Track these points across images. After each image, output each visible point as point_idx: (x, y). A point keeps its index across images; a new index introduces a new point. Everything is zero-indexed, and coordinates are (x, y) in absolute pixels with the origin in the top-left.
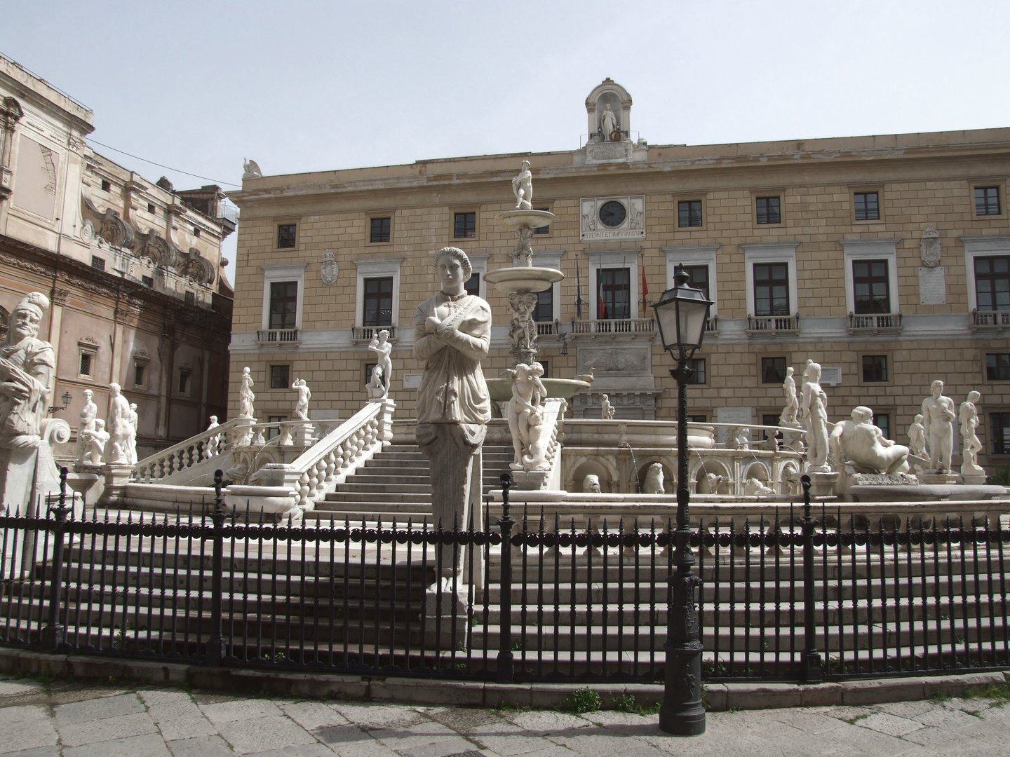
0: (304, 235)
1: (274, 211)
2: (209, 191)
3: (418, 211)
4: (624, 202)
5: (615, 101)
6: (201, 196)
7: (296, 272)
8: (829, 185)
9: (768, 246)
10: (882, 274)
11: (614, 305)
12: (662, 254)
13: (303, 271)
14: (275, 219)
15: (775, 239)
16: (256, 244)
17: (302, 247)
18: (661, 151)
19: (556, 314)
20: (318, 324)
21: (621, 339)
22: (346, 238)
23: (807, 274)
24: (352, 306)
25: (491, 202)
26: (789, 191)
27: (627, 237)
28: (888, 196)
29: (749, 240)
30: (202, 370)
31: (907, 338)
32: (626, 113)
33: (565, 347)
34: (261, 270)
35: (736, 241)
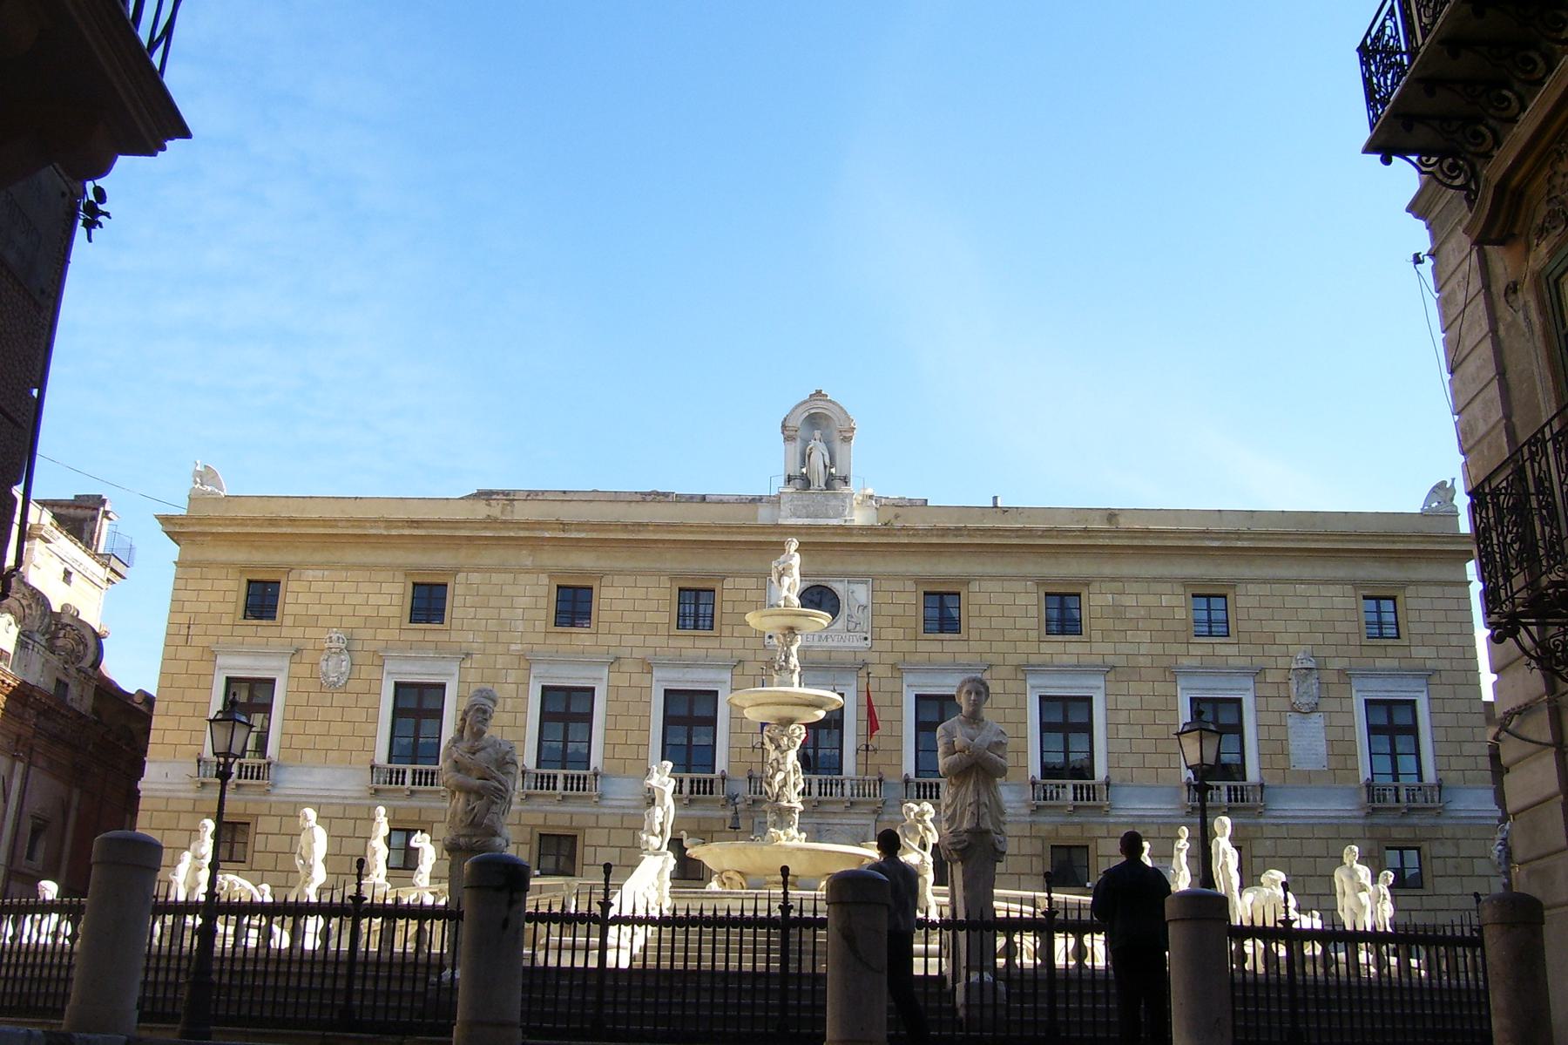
0: (291, 600)
1: (241, 555)
2: (90, 503)
3: (496, 578)
4: (839, 587)
5: (828, 426)
6: (71, 511)
7: (274, 663)
8: (1157, 580)
9: (1062, 670)
10: (1233, 720)
11: (816, 753)
12: (897, 674)
13: (287, 663)
14: (243, 569)
15: (1074, 660)
16: (204, 607)
17: (288, 621)
18: (898, 510)
19: (721, 764)
20: (307, 755)
21: (828, 808)
22: (368, 612)
23: (1122, 717)
24: (372, 727)
25: (620, 572)
26: (1095, 587)
27: (841, 644)
28: (1241, 602)
29: (1034, 659)
30: (65, 824)
31: (1272, 821)
32: (845, 446)
33: (736, 818)
34: (211, 655)
35: (1013, 659)
